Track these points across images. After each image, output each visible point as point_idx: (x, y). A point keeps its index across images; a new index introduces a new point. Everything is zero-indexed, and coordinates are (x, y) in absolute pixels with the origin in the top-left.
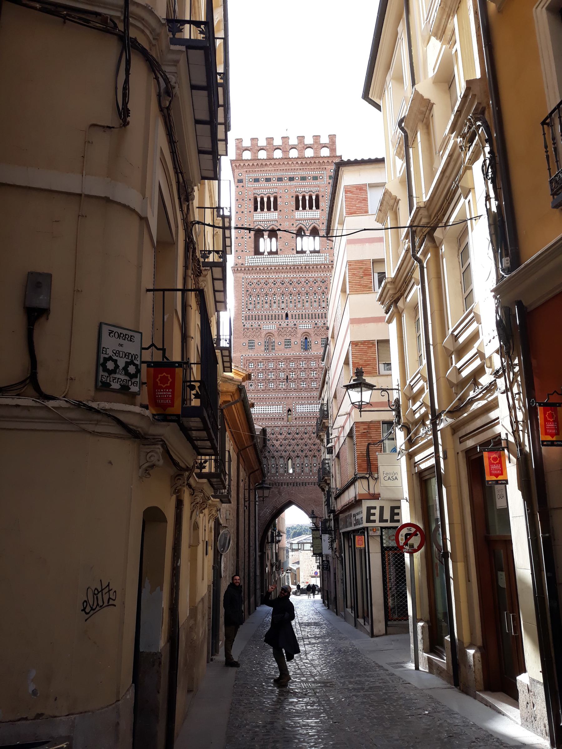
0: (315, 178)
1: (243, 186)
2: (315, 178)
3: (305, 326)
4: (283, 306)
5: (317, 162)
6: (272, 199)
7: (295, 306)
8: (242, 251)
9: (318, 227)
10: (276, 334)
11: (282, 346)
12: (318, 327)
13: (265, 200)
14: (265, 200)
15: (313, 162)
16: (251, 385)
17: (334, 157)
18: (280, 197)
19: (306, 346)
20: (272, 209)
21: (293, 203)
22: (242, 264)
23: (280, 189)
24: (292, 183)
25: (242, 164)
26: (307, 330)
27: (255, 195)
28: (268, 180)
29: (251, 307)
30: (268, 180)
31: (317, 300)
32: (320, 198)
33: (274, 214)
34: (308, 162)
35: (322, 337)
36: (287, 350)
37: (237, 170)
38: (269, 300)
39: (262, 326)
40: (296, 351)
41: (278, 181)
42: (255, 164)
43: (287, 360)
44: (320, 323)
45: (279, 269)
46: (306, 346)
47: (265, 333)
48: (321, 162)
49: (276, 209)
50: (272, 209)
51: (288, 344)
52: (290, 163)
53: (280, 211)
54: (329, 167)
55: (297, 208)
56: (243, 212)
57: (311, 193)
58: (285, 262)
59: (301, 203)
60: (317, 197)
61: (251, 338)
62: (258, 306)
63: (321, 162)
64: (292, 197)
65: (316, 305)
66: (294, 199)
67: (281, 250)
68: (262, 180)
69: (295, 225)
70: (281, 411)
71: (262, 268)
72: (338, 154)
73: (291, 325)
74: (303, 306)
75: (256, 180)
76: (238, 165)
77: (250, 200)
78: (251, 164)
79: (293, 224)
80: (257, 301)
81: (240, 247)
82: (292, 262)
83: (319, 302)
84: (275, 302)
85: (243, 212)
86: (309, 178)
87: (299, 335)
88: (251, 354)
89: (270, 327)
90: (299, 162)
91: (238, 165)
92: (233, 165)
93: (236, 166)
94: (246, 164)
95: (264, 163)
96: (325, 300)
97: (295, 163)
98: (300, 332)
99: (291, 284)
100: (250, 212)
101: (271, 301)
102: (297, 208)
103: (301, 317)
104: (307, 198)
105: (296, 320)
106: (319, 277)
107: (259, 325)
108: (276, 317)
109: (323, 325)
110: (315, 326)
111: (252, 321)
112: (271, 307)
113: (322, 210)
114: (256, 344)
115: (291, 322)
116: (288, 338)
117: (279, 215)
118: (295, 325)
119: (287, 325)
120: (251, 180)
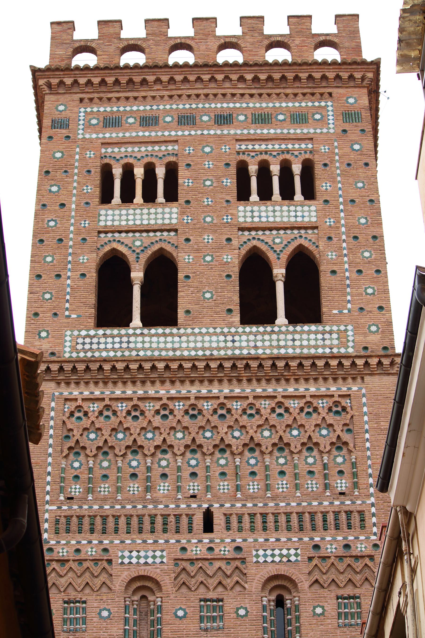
0: (299, 118)
1: (68, 137)
4: (194, 487)
5: (303, 75)
7: (238, 488)
9: (312, 248)
10: (167, 582)
12: (324, 558)
13: (139, 172)
14: (139, 172)
15: (290, 76)
17: (355, 63)
18: (188, 165)
20: (160, 198)
21: (230, 182)
22: (53, 354)
23: (186, 144)
25: (68, 81)
26: (283, 570)
27: (106, 161)
29: (76, 489)
30: (148, 121)
32: (318, 169)
33: (167, 210)
34: (277, 76)
35: (340, 592)
37: (53, 98)
38: (143, 468)
42: (110, 80)
44: (331, 543)
45: (177, 370)
47: (125, 575)
48: (317, 75)
49: (171, 195)
50: (160, 198)
52: (220, 77)
53: (188, 202)
54: (341, 91)
56: (63, 205)
57: (288, 157)
58: (203, 349)
59: (252, 181)
60: (308, 169)
61: (72, 594)
62: (105, 489)
63: (317, 75)
65: (313, 485)
66: (233, 170)
67: (188, 312)
69: (235, 243)
71: (120, 366)
72: (368, 55)
73: (225, 550)
74: (268, 487)
75: (112, 122)
76: (55, 81)
78: (96, 80)
79: (229, 240)
80: (98, 473)
82: (226, 348)
83: (326, 476)
84: (164, 476)
87: (254, 584)
89: (148, 554)
90: (249, 77)
91: (55, 81)
92: (41, 82)
93: (49, 85)
94: (82, 81)
95: (137, 79)
96: (346, 468)
97: (234, 77)
98: (256, 577)
99: (222, 416)
101: (149, 469)
102: (243, 195)
103: (263, 522)
104: (275, 169)
105: (244, 534)
106: (322, 397)
108: (171, 523)
109: (341, 552)
110: (312, 553)
111: (78, 537)
112: (147, 489)
113: (326, 201)
114: (91, 614)
115: (223, 542)
116: (212, 595)
117: (182, 213)
118: (238, 549)
119: (211, 549)
120: (94, 122)
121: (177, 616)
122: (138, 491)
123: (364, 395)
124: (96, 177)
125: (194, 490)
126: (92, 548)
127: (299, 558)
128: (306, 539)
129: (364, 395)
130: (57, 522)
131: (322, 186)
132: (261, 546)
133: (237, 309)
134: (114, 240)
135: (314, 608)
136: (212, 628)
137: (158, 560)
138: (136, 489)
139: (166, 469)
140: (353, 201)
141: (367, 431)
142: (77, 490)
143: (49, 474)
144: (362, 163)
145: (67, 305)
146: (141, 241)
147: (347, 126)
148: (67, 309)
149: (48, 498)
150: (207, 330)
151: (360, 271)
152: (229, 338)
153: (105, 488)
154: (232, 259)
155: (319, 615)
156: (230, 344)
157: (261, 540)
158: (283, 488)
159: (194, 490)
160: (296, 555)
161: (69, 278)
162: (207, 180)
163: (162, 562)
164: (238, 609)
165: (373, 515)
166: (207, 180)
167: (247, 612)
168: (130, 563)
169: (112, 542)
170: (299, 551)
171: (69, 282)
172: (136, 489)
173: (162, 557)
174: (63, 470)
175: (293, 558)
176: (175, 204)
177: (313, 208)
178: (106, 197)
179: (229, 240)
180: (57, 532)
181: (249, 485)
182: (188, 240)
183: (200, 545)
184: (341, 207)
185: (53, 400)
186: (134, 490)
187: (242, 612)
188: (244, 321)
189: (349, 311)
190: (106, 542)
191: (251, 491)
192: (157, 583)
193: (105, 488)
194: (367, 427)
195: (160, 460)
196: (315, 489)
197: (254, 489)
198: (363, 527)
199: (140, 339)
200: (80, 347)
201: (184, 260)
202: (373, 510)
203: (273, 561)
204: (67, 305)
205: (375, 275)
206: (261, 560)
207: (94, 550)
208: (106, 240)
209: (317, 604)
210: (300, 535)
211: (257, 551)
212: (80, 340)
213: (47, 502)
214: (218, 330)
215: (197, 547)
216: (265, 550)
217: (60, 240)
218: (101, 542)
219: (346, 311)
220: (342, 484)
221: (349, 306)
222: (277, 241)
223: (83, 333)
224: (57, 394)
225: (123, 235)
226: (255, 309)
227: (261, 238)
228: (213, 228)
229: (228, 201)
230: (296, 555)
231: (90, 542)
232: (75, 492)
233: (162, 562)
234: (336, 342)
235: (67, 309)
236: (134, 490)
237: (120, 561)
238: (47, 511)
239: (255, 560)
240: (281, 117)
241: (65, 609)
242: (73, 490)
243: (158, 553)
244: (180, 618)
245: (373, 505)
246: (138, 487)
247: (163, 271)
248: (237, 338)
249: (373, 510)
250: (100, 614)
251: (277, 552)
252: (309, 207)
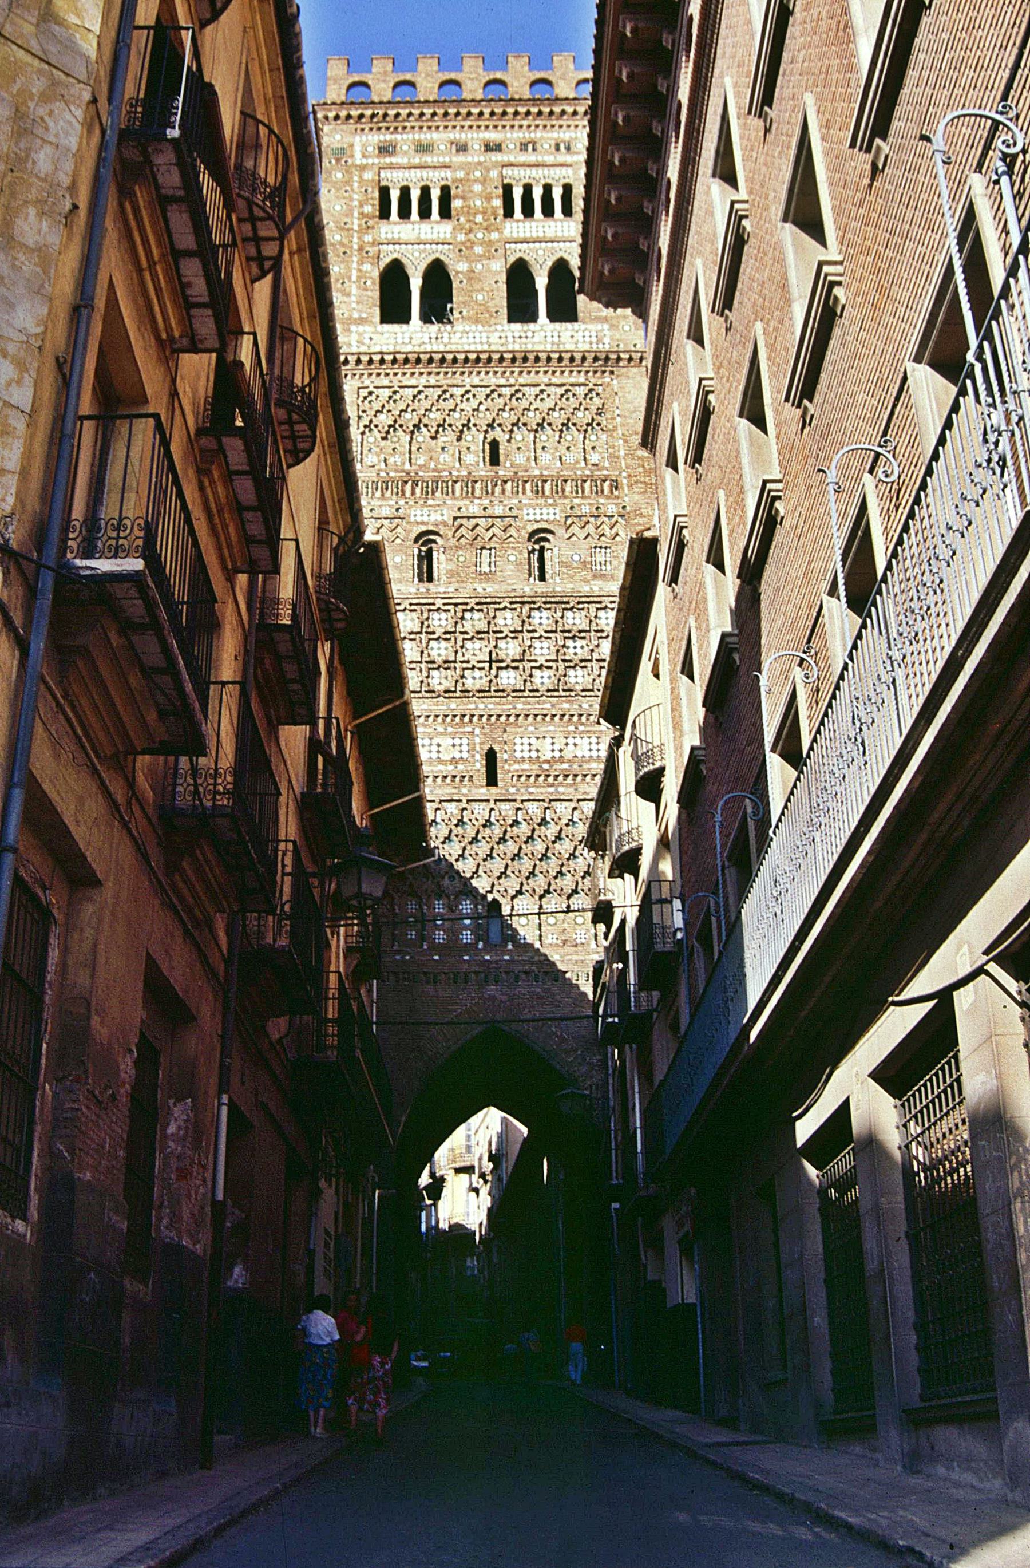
21: (498, 203)
24: (496, 157)
55: (509, 213)
70: (465, 755)
102: (509, 213)
133: (504, 312)
150: (480, 326)
154: (499, 268)
162: (478, 199)
166: (478, 199)
178: (384, 213)
188: (510, 321)
192: (437, 534)
201: (457, 267)
225: (403, 246)
226: (521, 309)
228: (482, 243)
247: (438, 277)
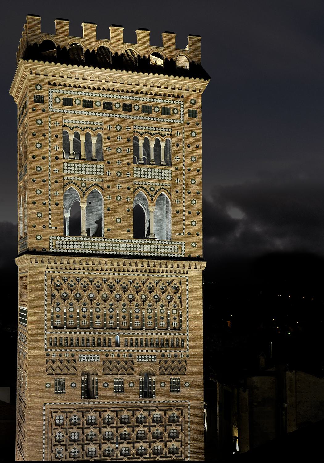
0: (166, 112)
2: (166, 112)
3: (146, 359)
6: (94, 140)
8: (44, 227)
11: (111, 390)
12: (166, 362)
16: (59, 453)
19: (147, 391)
21: (130, 152)
28: (87, 104)
29: (58, 322)
31: (164, 315)
36: (118, 396)
39: (77, 355)
40: (132, 397)
41: (104, 108)
43: (116, 411)
44: (170, 352)
46: (147, 391)
51: (119, 389)
56: (44, 158)
64: (129, 140)
68: (78, 102)
77: (56, 136)
79: (129, 189)
81: (40, 220)
83: (168, 321)
85: (44, 158)
86: (157, 109)
88: (60, 401)
100: (57, 158)
107: (73, 356)
117: (106, 168)
119: (119, 356)
120: (58, 100)
121: (104, 386)
122: (86, 324)
123: (187, 280)
124: (60, 139)
125: (111, 324)
126: (67, 353)
127: (156, 360)
128: (159, 351)
129: (187, 280)
130: (51, 339)
131: (176, 159)
132: (140, 354)
133: (132, 229)
134: (72, 183)
135: (161, 383)
136: (119, 392)
137: (96, 360)
138: (85, 323)
139: (99, 313)
140: (189, 170)
141: (187, 299)
142: (59, 323)
143: (46, 315)
144: (195, 145)
145: (50, 221)
146: (85, 183)
147: (190, 119)
148: (50, 224)
149: (46, 328)
151: (190, 213)
152: (128, 246)
153: (71, 322)
155: (163, 387)
156: (128, 249)
157: (140, 351)
158: (150, 324)
159: (111, 324)
160: (155, 358)
161: (50, 204)
163: (98, 361)
164: (130, 383)
165: (188, 340)
167: (134, 384)
168: (84, 361)
169: (76, 350)
170: (156, 357)
171: (50, 207)
172: (85, 323)
173: (98, 358)
174: (52, 314)
175: (153, 360)
176: (102, 163)
177: (170, 172)
179: (129, 189)
180: (51, 346)
181: (135, 323)
182: (109, 187)
183: (114, 352)
184: (184, 172)
185: (46, 275)
186: (84, 324)
187: (131, 385)
189: (184, 234)
190: (73, 350)
191: (136, 325)
193: (71, 322)
194: (187, 297)
195: (96, 308)
196: (163, 326)
197: (137, 324)
198: (183, 345)
199: (86, 244)
200: (57, 246)
202: (188, 338)
203: (145, 361)
204: (50, 221)
205: (197, 215)
206: (140, 360)
207: (68, 354)
208: (68, 181)
209: (162, 381)
210: (157, 349)
211: (138, 356)
212: (57, 242)
213: (46, 330)
214: (123, 241)
215: (113, 354)
216: (142, 356)
217: (44, 181)
218: (71, 350)
219: (182, 234)
220: (175, 324)
221: (184, 231)
222: (152, 189)
223: (59, 238)
224: (47, 272)
227: (145, 186)
229: (129, 164)
230: (155, 358)
231: (66, 350)
232: (58, 323)
233: (98, 361)
234: (176, 251)
235: (50, 224)
236: (84, 324)
237: (80, 360)
238: (46, 334)
239: (137, 360)
240: (157, 109)
241: (55, 383)
242: (57, 322)
243: (96, 356)
244: (106, 387)
245: (187, 335)
246: (86, 322)
248: (132, 246)
249: (188, 338)
250: (71, 385)
251: (147, 357)
252: (168, 170)
